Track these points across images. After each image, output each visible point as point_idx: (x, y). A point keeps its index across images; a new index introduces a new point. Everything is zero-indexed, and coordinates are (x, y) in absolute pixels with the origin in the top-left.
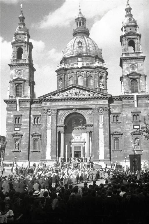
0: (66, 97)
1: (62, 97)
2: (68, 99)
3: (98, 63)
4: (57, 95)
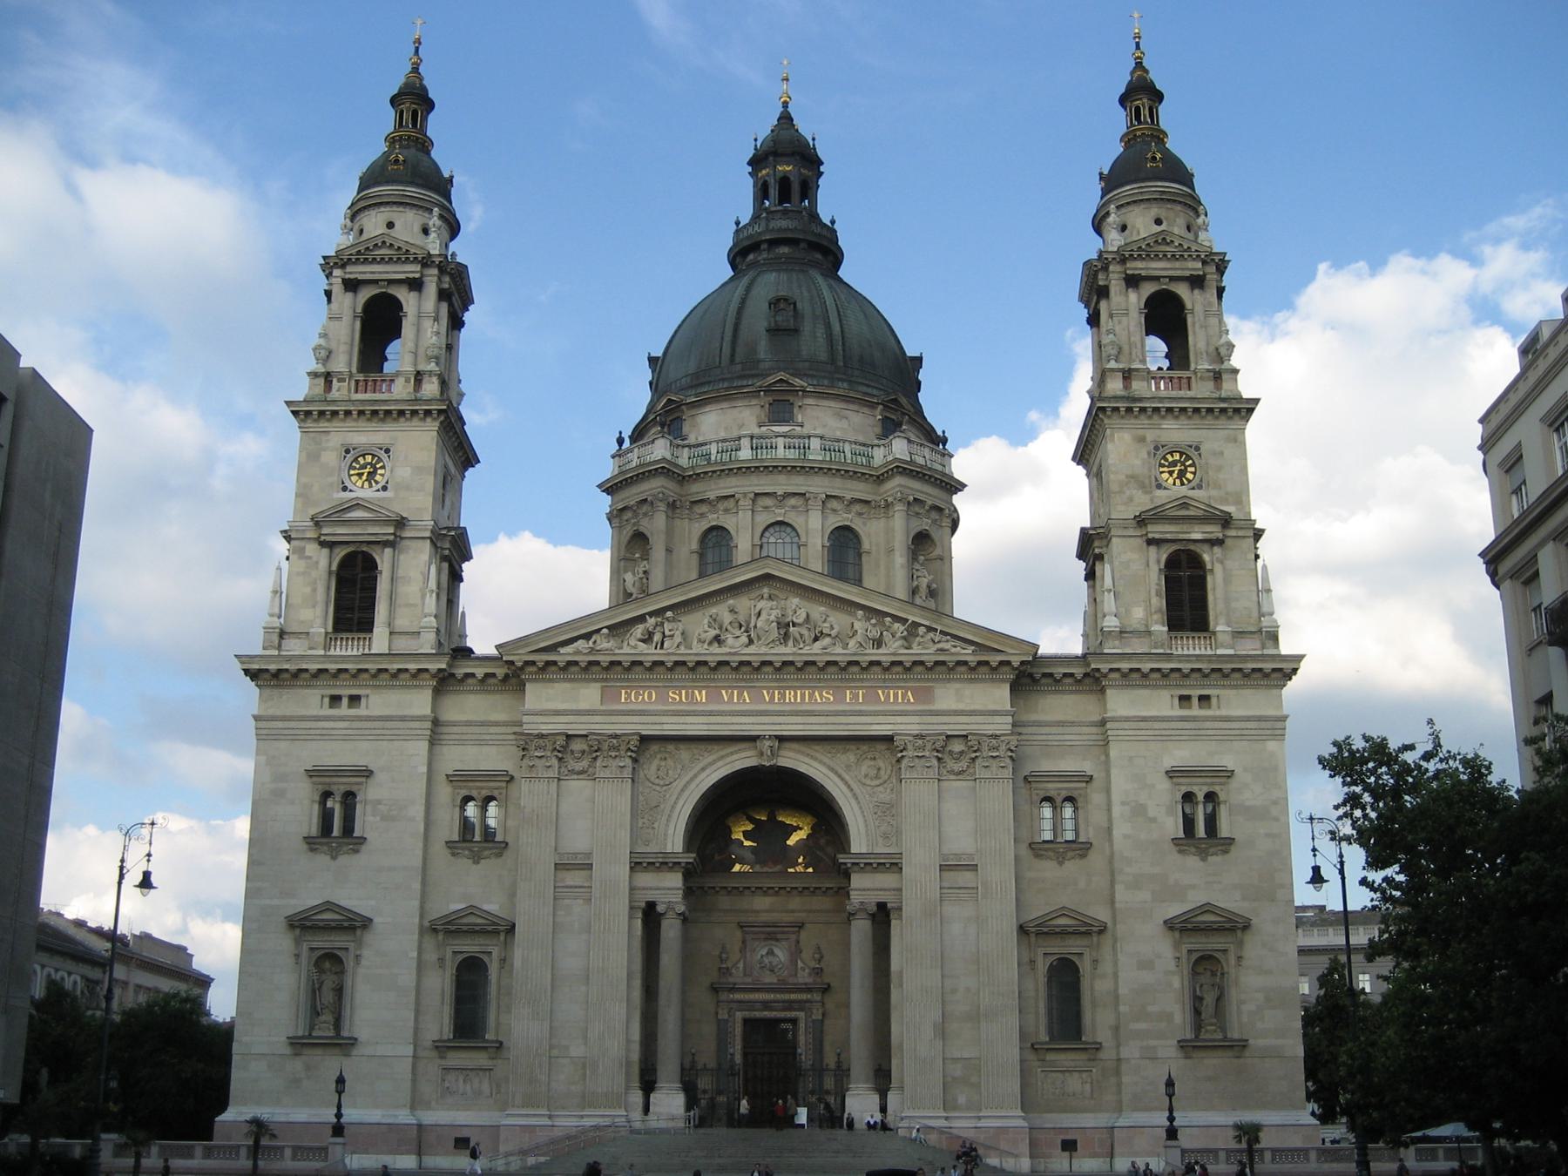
0: (697, 648)
1: (682, 650)
2: (720, 663)
3: (906, 441)
4: (639, 630)
